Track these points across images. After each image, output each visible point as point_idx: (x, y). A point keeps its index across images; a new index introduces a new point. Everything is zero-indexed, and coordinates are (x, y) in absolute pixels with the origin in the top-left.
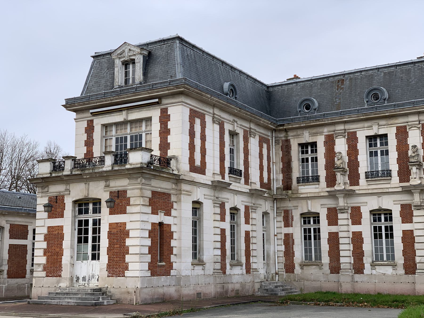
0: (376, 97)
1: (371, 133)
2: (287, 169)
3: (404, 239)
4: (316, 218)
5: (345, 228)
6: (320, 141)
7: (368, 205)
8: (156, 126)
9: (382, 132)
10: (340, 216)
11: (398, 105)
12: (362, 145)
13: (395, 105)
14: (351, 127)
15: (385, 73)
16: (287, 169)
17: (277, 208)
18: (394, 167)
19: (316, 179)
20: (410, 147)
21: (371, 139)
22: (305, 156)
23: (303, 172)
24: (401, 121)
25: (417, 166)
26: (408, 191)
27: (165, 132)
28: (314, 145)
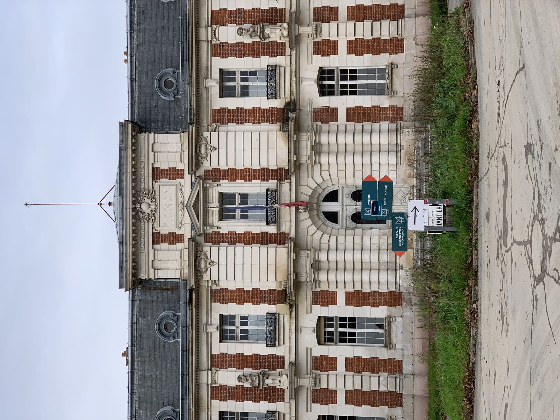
3: (357, 403)
11: (184, 394)
13: (183, 399)
15: (139, 408)
20: (240, 384)
24: (205, 393)
25: (265, 378)
26: (296, 392)
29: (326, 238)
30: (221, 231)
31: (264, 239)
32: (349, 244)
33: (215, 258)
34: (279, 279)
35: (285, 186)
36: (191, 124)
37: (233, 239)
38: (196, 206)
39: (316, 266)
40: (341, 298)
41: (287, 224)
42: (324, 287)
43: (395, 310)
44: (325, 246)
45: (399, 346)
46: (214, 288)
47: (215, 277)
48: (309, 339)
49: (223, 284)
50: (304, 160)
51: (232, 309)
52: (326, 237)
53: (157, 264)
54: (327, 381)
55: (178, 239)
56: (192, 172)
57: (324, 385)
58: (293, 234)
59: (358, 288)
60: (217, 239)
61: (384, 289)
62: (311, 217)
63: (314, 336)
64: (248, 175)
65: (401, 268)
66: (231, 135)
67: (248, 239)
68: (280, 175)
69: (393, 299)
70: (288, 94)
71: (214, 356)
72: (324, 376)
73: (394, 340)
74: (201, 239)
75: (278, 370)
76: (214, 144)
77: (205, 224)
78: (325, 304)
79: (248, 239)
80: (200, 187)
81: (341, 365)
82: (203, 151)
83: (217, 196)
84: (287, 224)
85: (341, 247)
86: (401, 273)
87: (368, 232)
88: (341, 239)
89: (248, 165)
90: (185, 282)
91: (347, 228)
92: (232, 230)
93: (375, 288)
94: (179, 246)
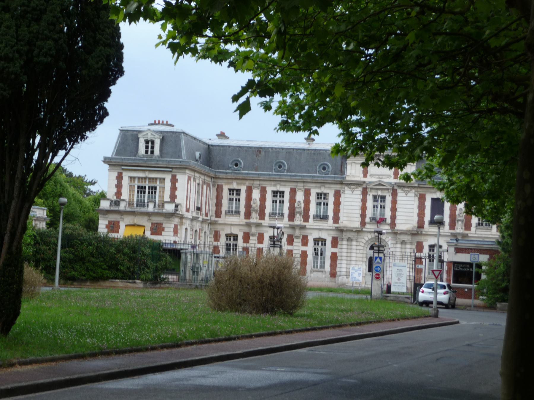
0: (280, 167)
1: (275, 189)
2: (219, 204)
4: (236, 237)
5: (253, 245)
6: (243, 189)
7: (268, 233)
8: (168, 184)
9: (281, 189)
10: (251, 238)
12: (269, 196)
14: (264, 184)
16: (219, 204)
17: (210, 229)
18: (286, 212)
19: (238, 213)
20: (297, 201)
21: (275, 193)
22: (231, 197)
23: (229, 207)
27: (174, 189)
28: (238, 191)
29: (362, 244)
30: (368, 196)
31: (363, 216)
32: (358, 255)
33: (355, 192)
34: (344, 222)
35: (388, 227)
36: (419, 184)
37: (364, 201)
38: (380, 184)
39: (349, 240)
40: (334, 250)
41: (370, 227)
42: (340, 243)
43: (328, 274)
44: (358, 244)
45: (312, 275)
46: (341, 191)
47: (346, 192)
48: (316, 235)
49: (342, 195)
50: (399, 237)
51: (331, 200)
52: (363, 245)
53: (353, 164)
54: (297, 242)
55: (365, 175)
56: (396, 184)
57: (295, 240)
58: (364, 229)
59: (339, 258)
60: (365, 193)
61: (338, 269)
62: (372, 238)
63: (317, 237)
64: (394, 209)
65: (347, 278)
66: (412, 203)
67: (364, 208)
68: (393, 224)
69: (333, 274)
70: (430, 230)
71: (310, 190)
72: (300, 240)
73: (315, 273)
74: (364, 186)
75: (302, 219)
76: (409, 195)
77: (371, 189)
78: (332, 242)
79: (364, 208)
80: (388, 187)
81: (304, 248)
82: (406, 189)
83: (384, 194)
84: (370, 227)
85: (358, 251)
86: (345, 277)
87: (364, 264)
88: (361, 251)
89: (398, 210)
90: (344, 178)
91: (366, 254)
92: (368, 201)
93: (338, 266)
94: (362, 175)
